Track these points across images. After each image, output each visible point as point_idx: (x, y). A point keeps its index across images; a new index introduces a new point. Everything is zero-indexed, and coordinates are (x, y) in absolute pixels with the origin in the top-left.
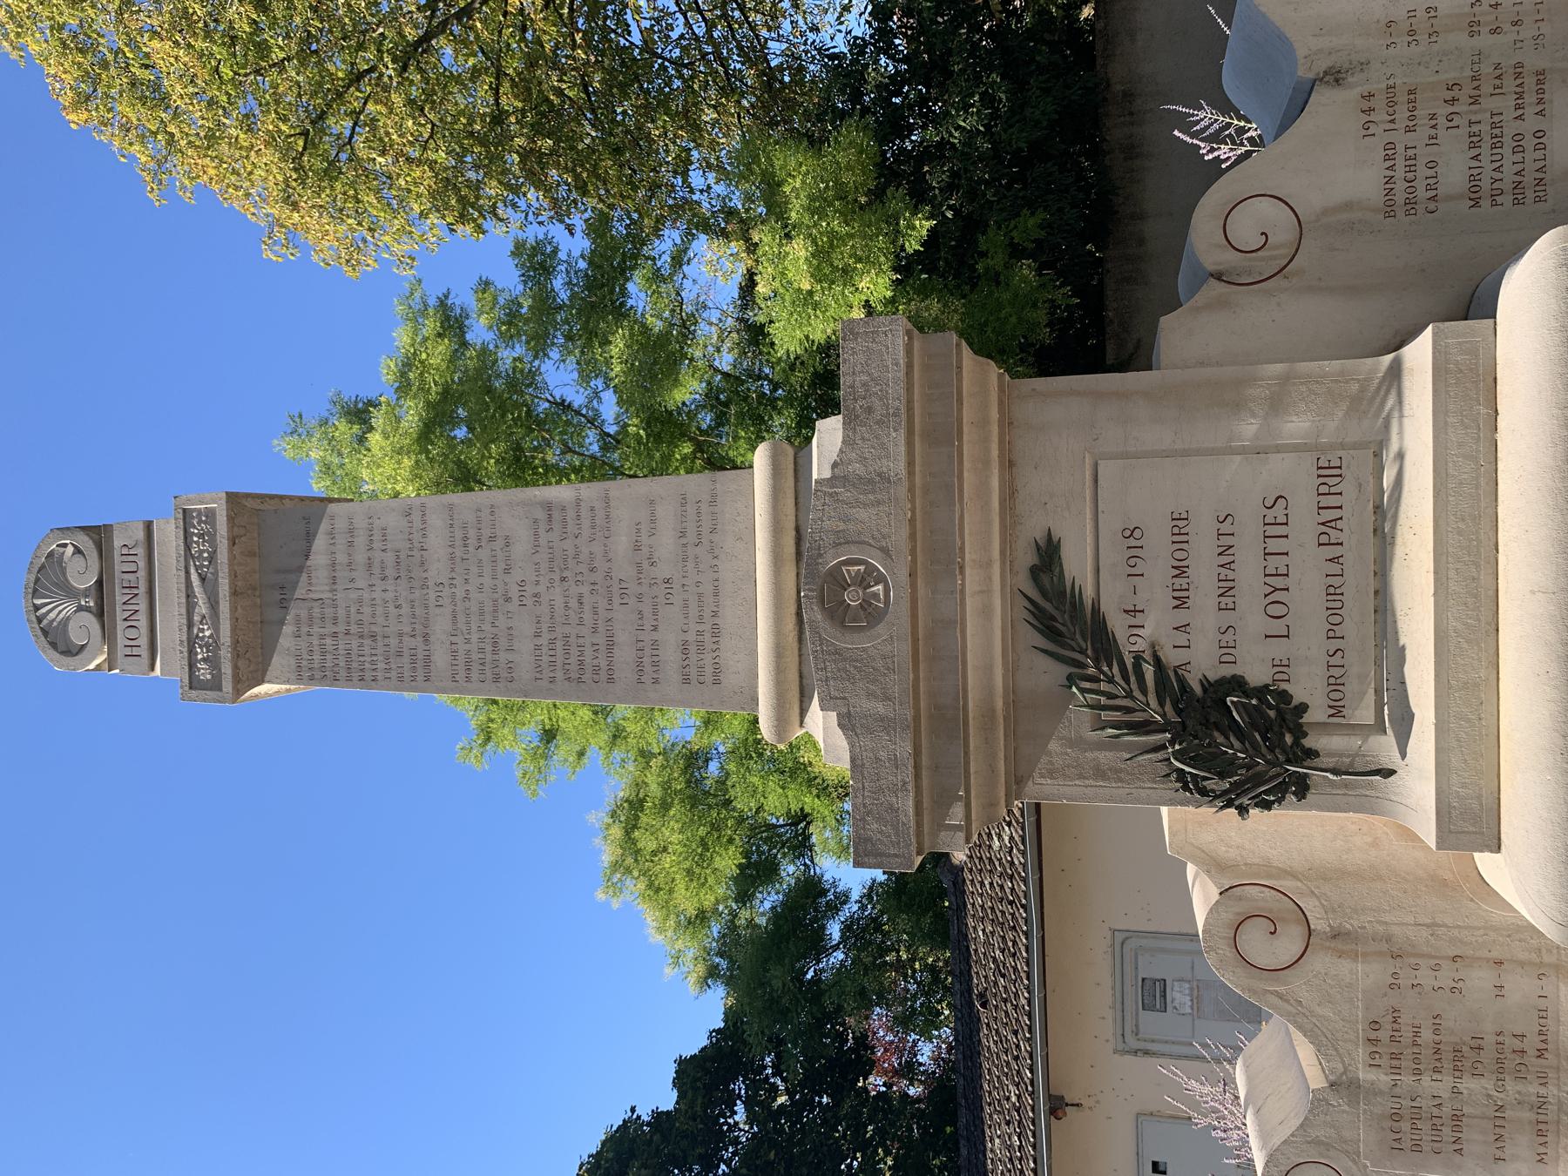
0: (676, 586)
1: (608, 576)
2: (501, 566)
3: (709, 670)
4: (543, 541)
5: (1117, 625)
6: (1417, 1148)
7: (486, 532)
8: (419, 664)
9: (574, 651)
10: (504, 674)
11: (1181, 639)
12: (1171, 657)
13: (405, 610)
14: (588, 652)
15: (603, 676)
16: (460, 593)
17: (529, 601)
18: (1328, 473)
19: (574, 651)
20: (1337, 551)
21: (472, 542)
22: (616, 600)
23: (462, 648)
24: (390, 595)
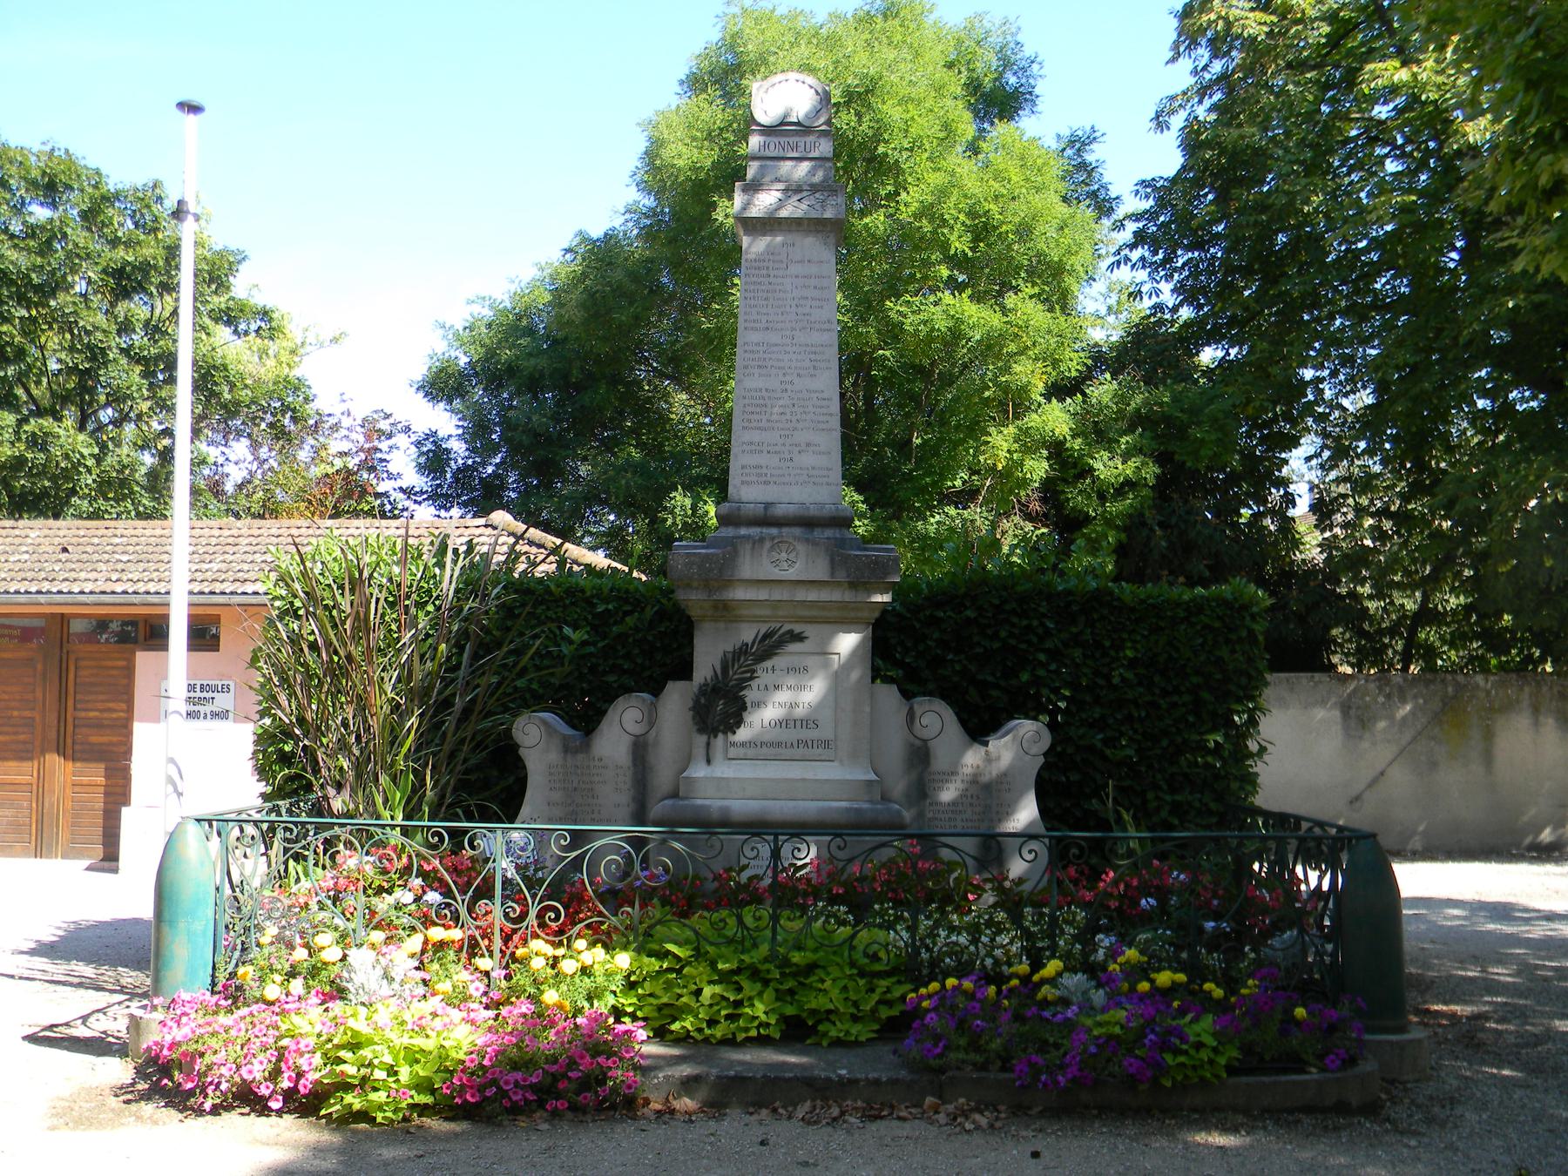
0: (789, 464)
1: (795, 429)
2: (801, 372)
3: (748, 479)
4: (813, 395)
5: (768, 664)
6: (551, 774)
7: (817, 364)
8: (752, 325)
9: (758, 410)
10: (747, 371)
11: (762, 687)
12: (754, 684)
13: (780, 318)
14: (756, 417)
15: (746, 424)
16: (788, 349)
17: (783, 387)
18: (826, 744)
19: (758, 410)
20: (795, 745)
21: (813, 356)
22: (783, 433)
23: (761, 348)
24: (788, 309)
